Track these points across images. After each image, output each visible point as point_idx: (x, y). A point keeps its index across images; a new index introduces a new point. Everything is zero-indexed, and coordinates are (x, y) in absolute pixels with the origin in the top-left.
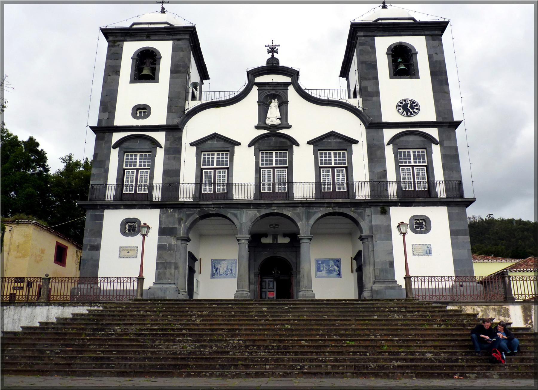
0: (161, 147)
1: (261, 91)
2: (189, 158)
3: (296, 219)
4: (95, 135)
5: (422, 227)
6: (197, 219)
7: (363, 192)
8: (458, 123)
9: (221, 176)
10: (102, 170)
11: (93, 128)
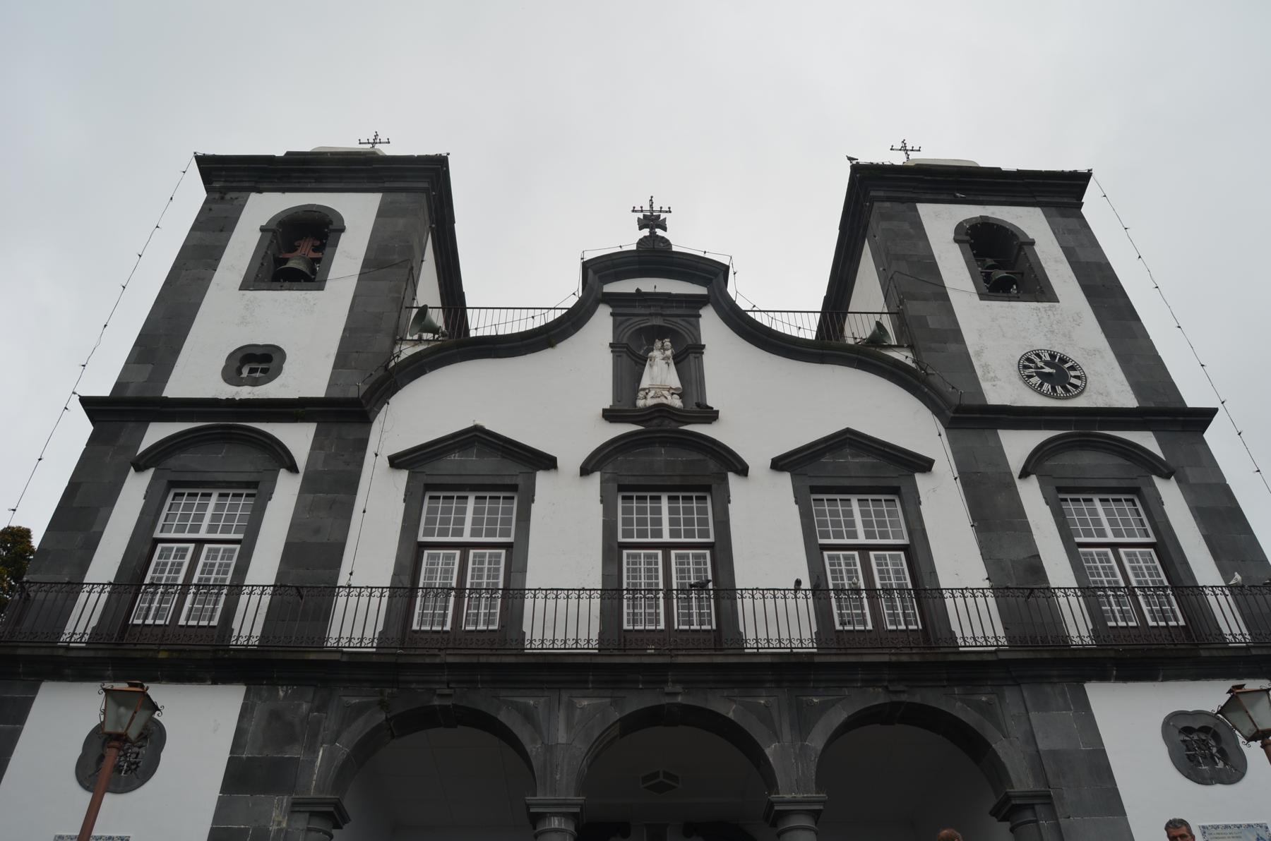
0: (293, 468)
1: (620, 318)
2: (380, 500)
3: (757, 731)
4: (89, 428)
6: (378, 729)
8: (1206, 416)
9: (487, 570)
11: (89, 404)
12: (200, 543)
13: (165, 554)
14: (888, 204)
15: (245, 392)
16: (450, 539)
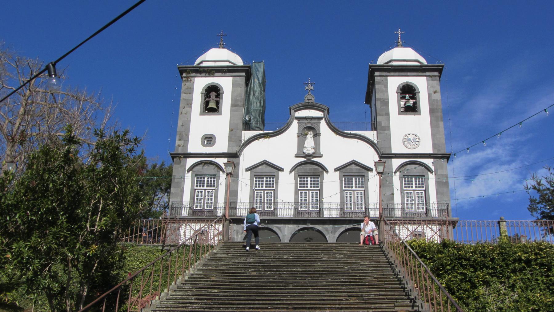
2: (245, 179)
12: (205, 189)
13: (198, 192)
14: (379, 78)
16: (261, 188)
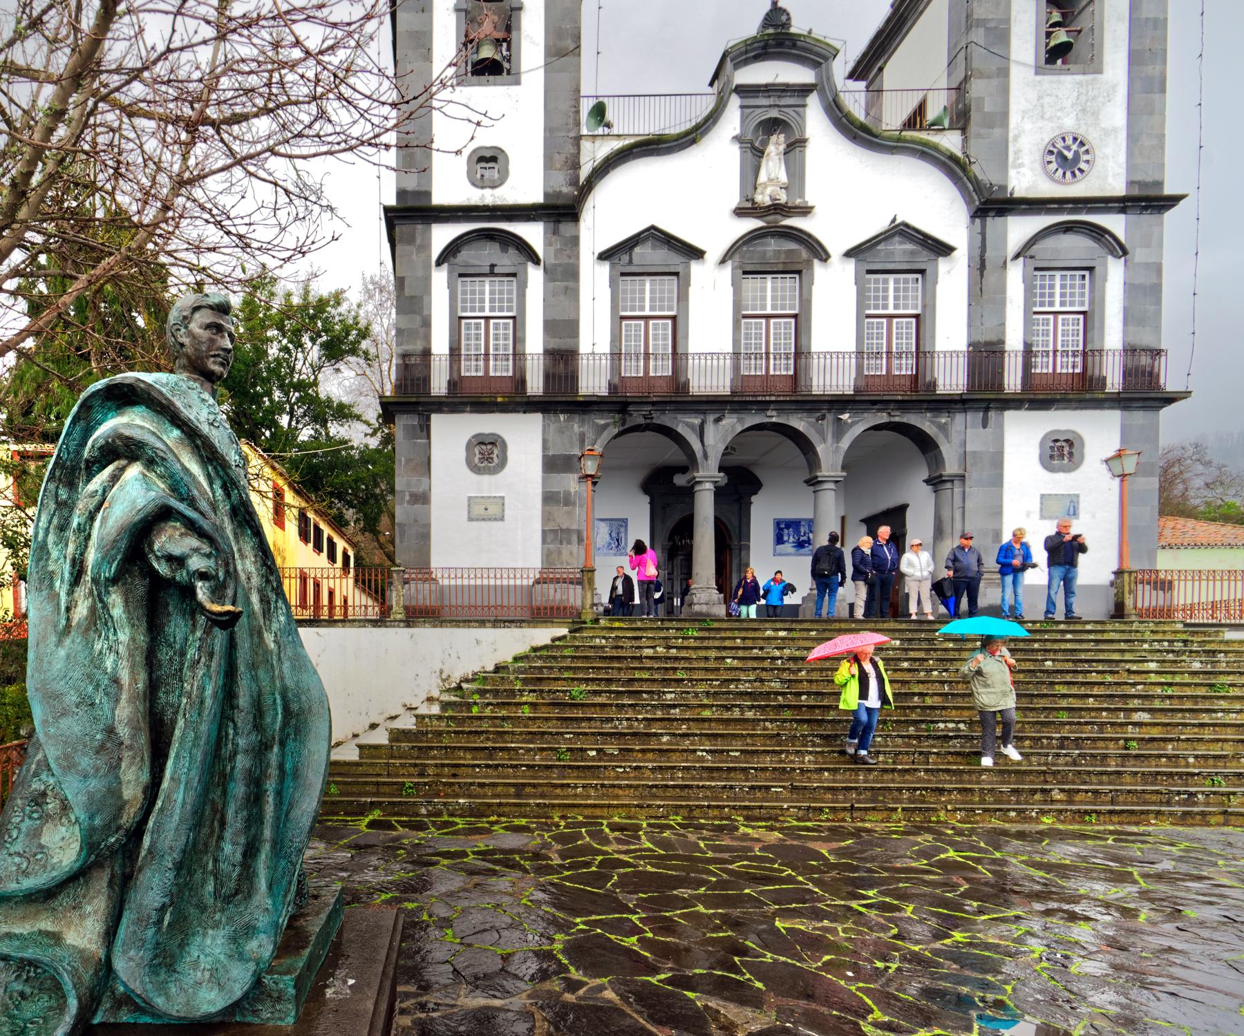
1: (748, 111)
5: (1062, 456)
7: (951, 378)
10: (418, 318)
15: (489, 197)
